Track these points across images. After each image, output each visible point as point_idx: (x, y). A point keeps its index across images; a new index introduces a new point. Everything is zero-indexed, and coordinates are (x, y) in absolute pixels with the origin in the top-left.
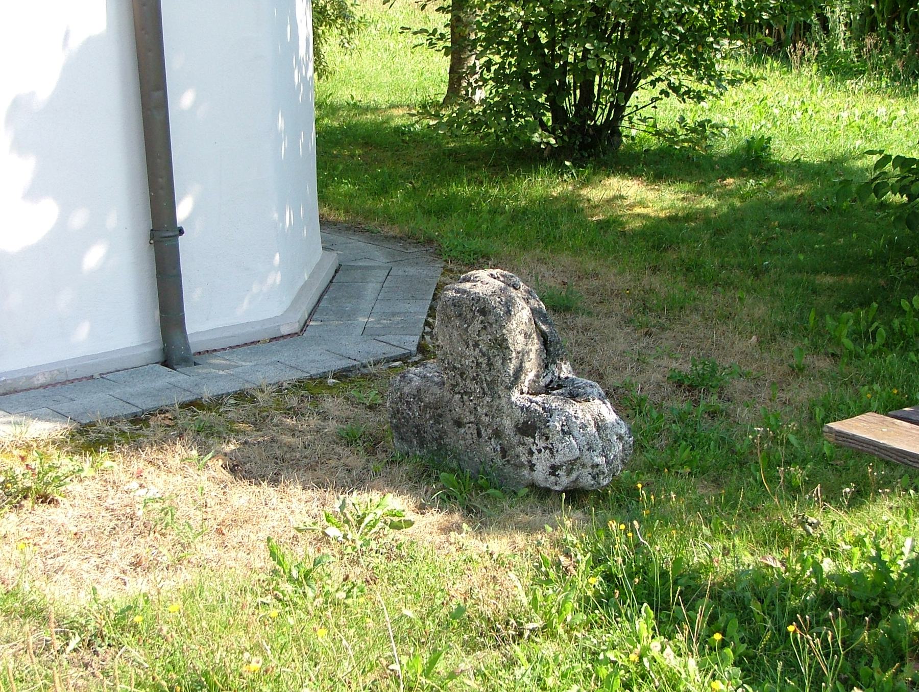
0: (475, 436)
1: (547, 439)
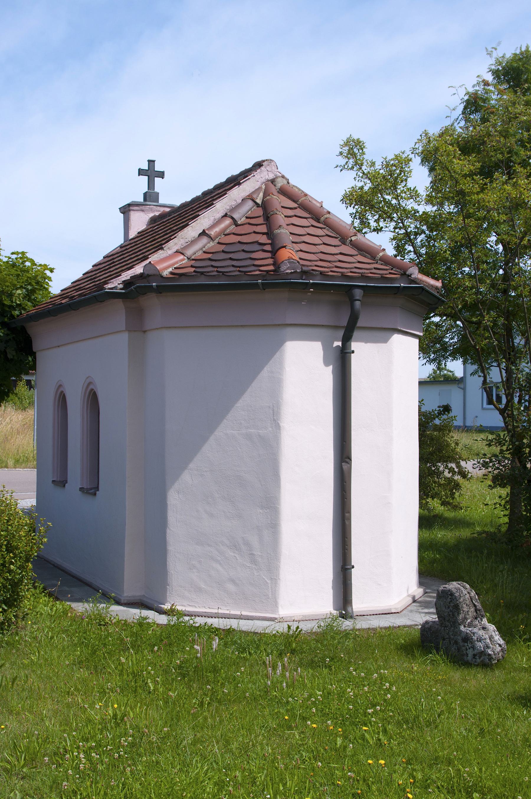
0: (449, 644)
1: (472, 643)
